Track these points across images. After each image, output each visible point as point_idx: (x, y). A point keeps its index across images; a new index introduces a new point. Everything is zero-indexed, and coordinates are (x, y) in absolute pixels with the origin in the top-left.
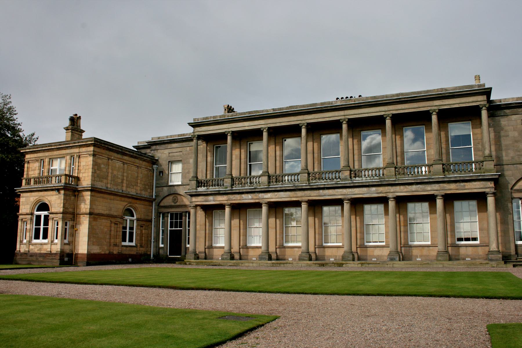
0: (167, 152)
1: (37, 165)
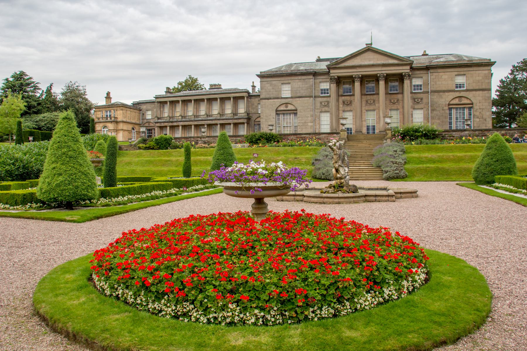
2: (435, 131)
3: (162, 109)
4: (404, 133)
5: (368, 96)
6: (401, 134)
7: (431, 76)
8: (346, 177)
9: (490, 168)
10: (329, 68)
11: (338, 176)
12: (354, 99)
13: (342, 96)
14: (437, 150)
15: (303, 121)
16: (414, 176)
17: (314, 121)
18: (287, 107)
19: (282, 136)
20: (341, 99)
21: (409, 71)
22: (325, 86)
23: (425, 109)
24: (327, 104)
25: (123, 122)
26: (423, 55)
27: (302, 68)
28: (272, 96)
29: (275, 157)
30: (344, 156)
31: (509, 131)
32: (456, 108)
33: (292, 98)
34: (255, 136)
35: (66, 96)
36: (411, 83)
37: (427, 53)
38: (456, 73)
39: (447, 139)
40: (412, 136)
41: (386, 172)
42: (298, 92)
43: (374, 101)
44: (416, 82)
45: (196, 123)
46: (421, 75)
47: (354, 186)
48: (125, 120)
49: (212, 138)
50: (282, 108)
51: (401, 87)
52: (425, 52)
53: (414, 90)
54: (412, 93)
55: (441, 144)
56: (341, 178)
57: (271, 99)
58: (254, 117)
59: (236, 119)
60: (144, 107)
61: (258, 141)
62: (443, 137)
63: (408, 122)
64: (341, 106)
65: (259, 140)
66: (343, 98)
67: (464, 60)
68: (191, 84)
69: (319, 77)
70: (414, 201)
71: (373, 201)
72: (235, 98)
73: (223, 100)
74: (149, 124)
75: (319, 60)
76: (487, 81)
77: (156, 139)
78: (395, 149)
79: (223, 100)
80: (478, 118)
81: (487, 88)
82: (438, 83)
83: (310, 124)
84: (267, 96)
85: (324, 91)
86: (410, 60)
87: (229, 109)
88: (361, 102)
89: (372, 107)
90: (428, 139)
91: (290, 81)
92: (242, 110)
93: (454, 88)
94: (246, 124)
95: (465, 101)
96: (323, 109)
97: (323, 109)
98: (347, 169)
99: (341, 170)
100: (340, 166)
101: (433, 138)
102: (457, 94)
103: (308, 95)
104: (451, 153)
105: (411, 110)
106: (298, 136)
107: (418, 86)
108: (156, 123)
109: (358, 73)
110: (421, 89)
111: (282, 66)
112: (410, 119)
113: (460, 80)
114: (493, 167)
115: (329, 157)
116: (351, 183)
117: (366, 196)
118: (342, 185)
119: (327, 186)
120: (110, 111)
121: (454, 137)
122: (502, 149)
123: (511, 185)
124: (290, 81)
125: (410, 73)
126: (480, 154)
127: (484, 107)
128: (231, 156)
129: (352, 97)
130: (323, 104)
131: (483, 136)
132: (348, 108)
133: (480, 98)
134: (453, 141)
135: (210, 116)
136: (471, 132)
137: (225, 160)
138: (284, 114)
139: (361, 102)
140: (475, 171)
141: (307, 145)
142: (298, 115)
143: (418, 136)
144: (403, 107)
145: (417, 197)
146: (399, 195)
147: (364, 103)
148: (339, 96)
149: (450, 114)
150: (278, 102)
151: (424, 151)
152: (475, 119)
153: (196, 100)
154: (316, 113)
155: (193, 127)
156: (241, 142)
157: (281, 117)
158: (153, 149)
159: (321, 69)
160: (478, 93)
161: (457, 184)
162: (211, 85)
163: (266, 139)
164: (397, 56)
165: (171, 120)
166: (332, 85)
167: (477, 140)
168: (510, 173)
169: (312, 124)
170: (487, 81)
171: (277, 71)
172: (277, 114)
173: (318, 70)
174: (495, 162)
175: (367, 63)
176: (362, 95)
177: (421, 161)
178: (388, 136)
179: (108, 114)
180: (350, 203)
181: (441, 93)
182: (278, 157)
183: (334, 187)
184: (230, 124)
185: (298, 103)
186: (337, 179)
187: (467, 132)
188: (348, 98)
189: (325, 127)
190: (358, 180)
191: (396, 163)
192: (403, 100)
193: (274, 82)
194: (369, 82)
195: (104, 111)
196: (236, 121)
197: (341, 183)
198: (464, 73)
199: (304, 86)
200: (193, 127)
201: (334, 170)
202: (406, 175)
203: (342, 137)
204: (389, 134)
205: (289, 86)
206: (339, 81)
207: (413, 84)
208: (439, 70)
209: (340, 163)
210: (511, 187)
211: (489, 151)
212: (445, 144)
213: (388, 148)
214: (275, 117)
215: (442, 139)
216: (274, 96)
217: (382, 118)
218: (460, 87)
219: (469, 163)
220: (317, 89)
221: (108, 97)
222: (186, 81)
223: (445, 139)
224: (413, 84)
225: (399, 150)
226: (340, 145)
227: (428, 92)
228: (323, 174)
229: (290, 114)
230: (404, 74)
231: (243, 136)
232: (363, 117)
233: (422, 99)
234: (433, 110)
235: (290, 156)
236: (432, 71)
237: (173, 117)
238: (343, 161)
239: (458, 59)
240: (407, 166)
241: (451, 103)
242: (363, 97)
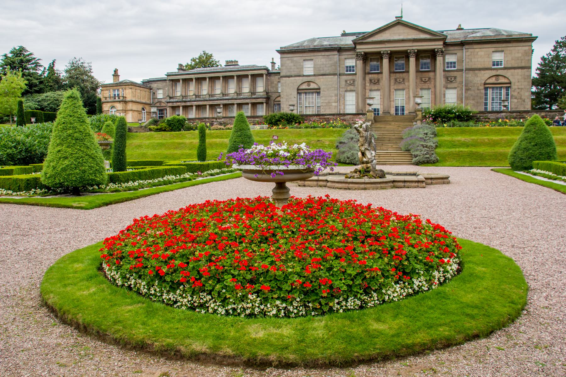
0: (156, 85)
1: (107, 92)
2: (470, 112)
3: (174, 88)
4: (436, 115)
5: (397, 74)
6: (433, 115)
7: (466, 52)
8: (372, 161)
9: (528, 153)
10: (355, 43)
11: (365, 159)
12: (382, 78)
13: (369, 73)
14: (471, 133)
15: (327, 101)
16: (445, 160)
17: (338, 101)
18: (309, 85)
19: (304, 117)
20: (368, 77)
21: (442, 47)
22: (351, 62)
23: (459, 89)
24: (353, 83)
25: (132, 101)
26: (458, 29)
27: (325, 43)
28: (293, 74)
29: (296, 139)
30: (371, 139)
31: (550, 113)
32: (493, 88)
33: (314, 75)
34: (274, 117)
35: (70, 74)
36: (444, 60)
37: (462, 27)
38: (493, 49)
39: (482, 121)
40: (444, 118)
41: (416, 156)
42: (321, 69)
43: (403, 80)
44: (450, 59)
45: (211, 103)
46: (455, 52)
47: (381, 171)
48: (134, 99)
49: (228, 119)
50: (304, 86)
51: (433, 64)
52: (460, 25)
53: (448, 67)
54: (444, 71)
55: (475, 126)
56: (367, 162)
57: (292, 76)
58: (274, 96)
59: (255, 98)
60: (154, 85)
61: (278, 123)
62: (477, 119)
63: (440, 102)
64: (368, 84)
65: (279, 121)
66: (370, 76)
67: (503, 35)
68: (205, 61)
69: (344, 53)
70: (445, 187)
71: (401, 187)
72: (253, 76)
73: (240, 78)
74: (160, 104)
75: (344, 34)
76: (527, 58)
77: (168, 121)
78: (426, 132)
79: (240, 78)
80: (516, 98)
81: (527, 65)
82: (473, 60)
83: (334, 104)
84: (288, 74)
85: (349, 68)
86: (443, 35)
87: (246, 88)
88: (390, 80)
89: (401, 87)
90: (461, 121)
91: (312, 58)
92: (260, 88)
93: (490, 65)
94: (265, 104)
95: (502, 80)
96: (349, 88)
97: (349, 88)
98: (373, 152)
99: (368, 153)
100: (366, 149)
101: (467, 120)
102: (494, 73)
103: (332, 72)
104: (485, 136)
105: (443, 89)
106: (321, 117)
107: (451, 63)
108: (167, 103)
109: (387, 49)
110: (454, 67)
111: (305, 41)
112: (443, 99)
113: (498, 57)
114: (531, 151)
115: (355, 140)
116: (378, 167)
117: (394, 181)
118: (368, 170)
119: (353, 170)
120: (118, 90)
121: (489, 119)
122: (542, 132)
123: (551, 171)
124: (312, 58)
125: (444, 49)
126: (518, 137)
127: (523, 87)
128: (249, 138)
129: (380, 75)
130: (348, 82)
131: (521, 118)
132: (376, 87)
133: (519, 77)
134: (488, 124)
135: (226, 95)
136: (509, 114)
137: (242, 143)
138: (306, 93)
139: (390, 80)
140: (511, 156)
141: (330, 127)
142: (321, 95)
143: (451, 118)
144: (435, 87)
145: (449, 183)
146: (429, 181)
147: (393, 81)
148: (365, 73)
149: (486, 94)
150: (300, 80)
151: (457, 133)
152: (512, 100)
153: (211, 78)
154: (341, 93)
155: (208, 107)
156: (259, 123)
157: (303, 96)
158: (165, 130)
159: (346, 45)
160: (516, 71)
161: (492, 170)
162: (227, 62)
163: (287, 120)
164: (429, 30)
165: (184, 100)
166: (358, 62)
167: (514, 123)
168: (549, 158)
169: (336, 104)
170: (527, 58)
171: (298, 47)
172: (298, 93)
173: (343, 45)
174: (534, 146)
175: (396, 37)
176: (391, 72)
177: (453, 145)
178: (418, 118)
179: (116, 93)
180: (377, 189)
181: (477, 72)
182: (300, 140)
183: (360, 171)
184: (247, 104)
185: (321, 82)
186: (363, 163)
187: (504, 114)
188: (375, 76)
189: (350, 107)
190: (385, 164)
191: (426, 147)
192: (435, 79)
193: (295, 59)
194: (398, 58)
195: (111, 90)
196: (254, 101)
197: (368, 168)
198: (503, 49)
199: (327, 62)
200: (208, 107)
201: (360, 154)
202: (437, 159)
203: (369, 118)
204: (420, 115)
205: (312, 62)
206: (366, 57)
207: (447, 61)
208: (475, 46)
209: (366, 146)
210: (550, 174)
211: (527, 135)
212: (480, 127)
213: (418, 130)
214: (296, 96)
215: (476, 121)
216: (296, 73)
217: (412, 98)
218: (497, 65)
219: (505, 147)
220: (341, 66)
221: (116, 74)
222: (200, 58)
223: (479, 121)
224: (447, 61)
225: (430, 133)
226: (367, 126)
227: (462, 70)
228: (348, 158)
229: (313, 93)
230: (436, 50)
231: (262, 116)
232: (392, 96)
233: (455, 78)
234: (467, 90)
235: (312, 139)
236: (467, 47)
237: (185, 96)
238: (370, 143)
239: (495, 34)
240: (438, 150)
241: (487, 82)
242: (392, 75)
